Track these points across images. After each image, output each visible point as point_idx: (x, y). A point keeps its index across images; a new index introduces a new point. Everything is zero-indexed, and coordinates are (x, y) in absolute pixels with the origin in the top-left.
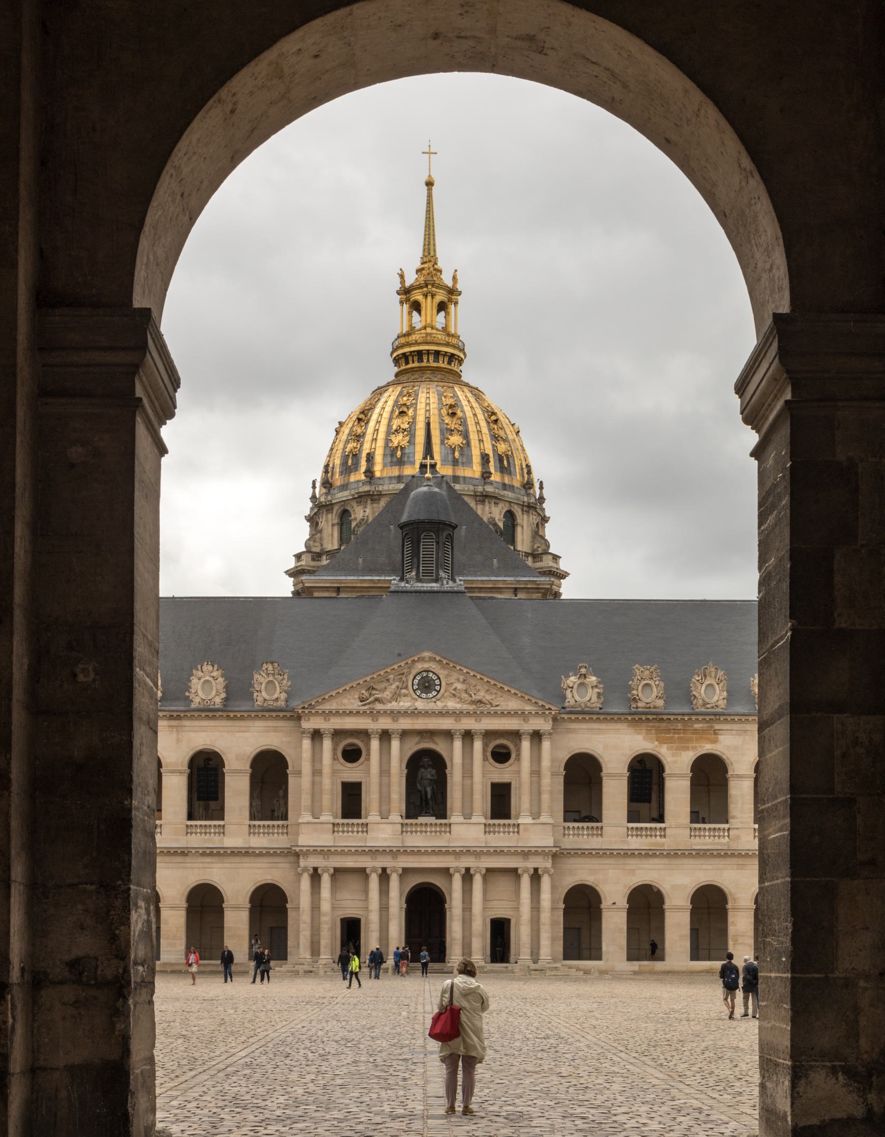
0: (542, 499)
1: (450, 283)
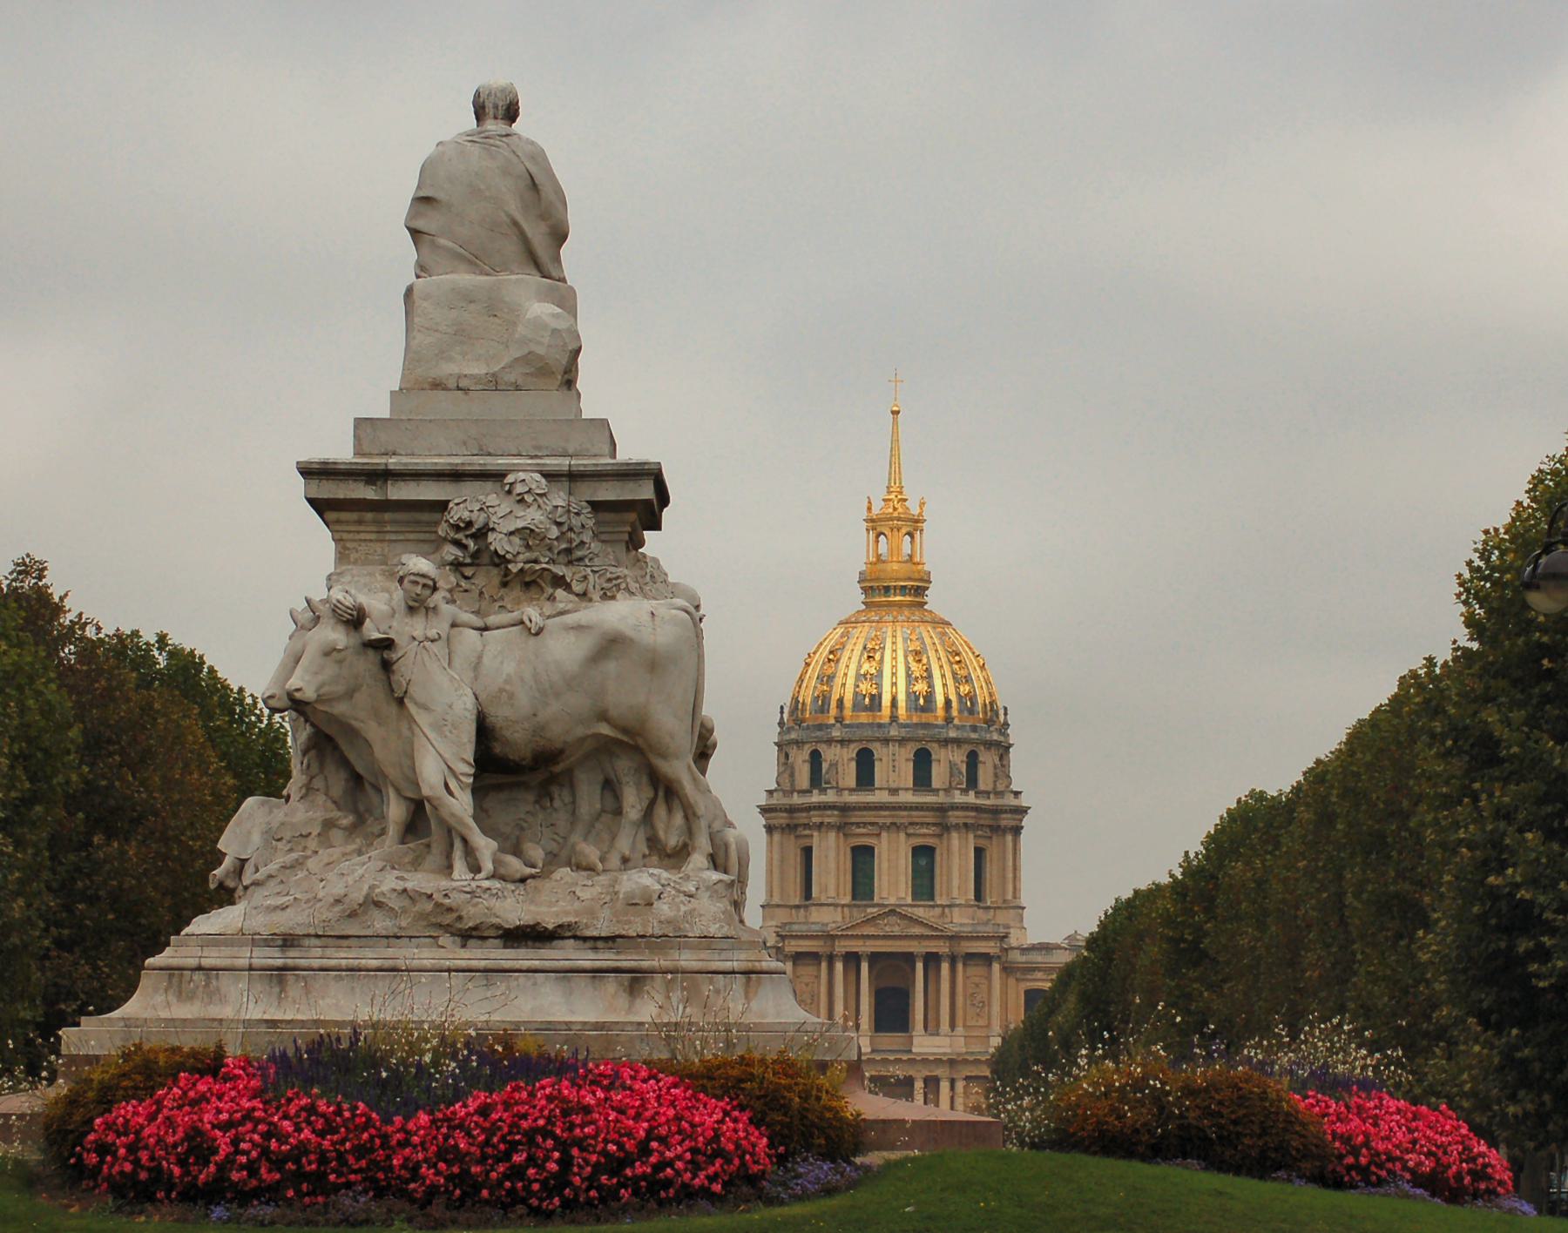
0: (1006, 725)
1: (915, 511)
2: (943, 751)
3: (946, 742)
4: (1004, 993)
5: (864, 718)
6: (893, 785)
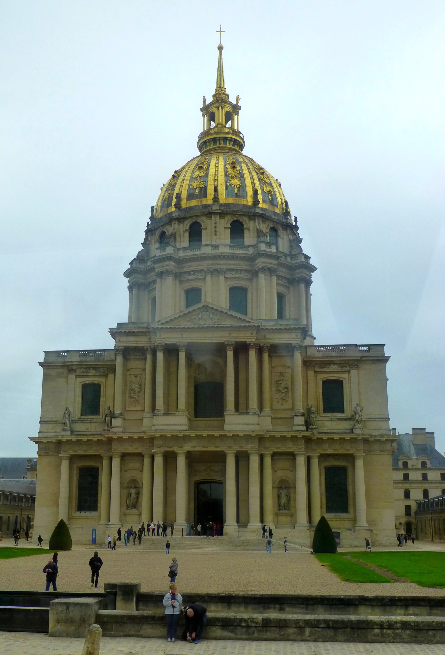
0: (296, 228)
1: (235, 103)
2: (252, 223)
4: (306, 382)
6: (214, 242)
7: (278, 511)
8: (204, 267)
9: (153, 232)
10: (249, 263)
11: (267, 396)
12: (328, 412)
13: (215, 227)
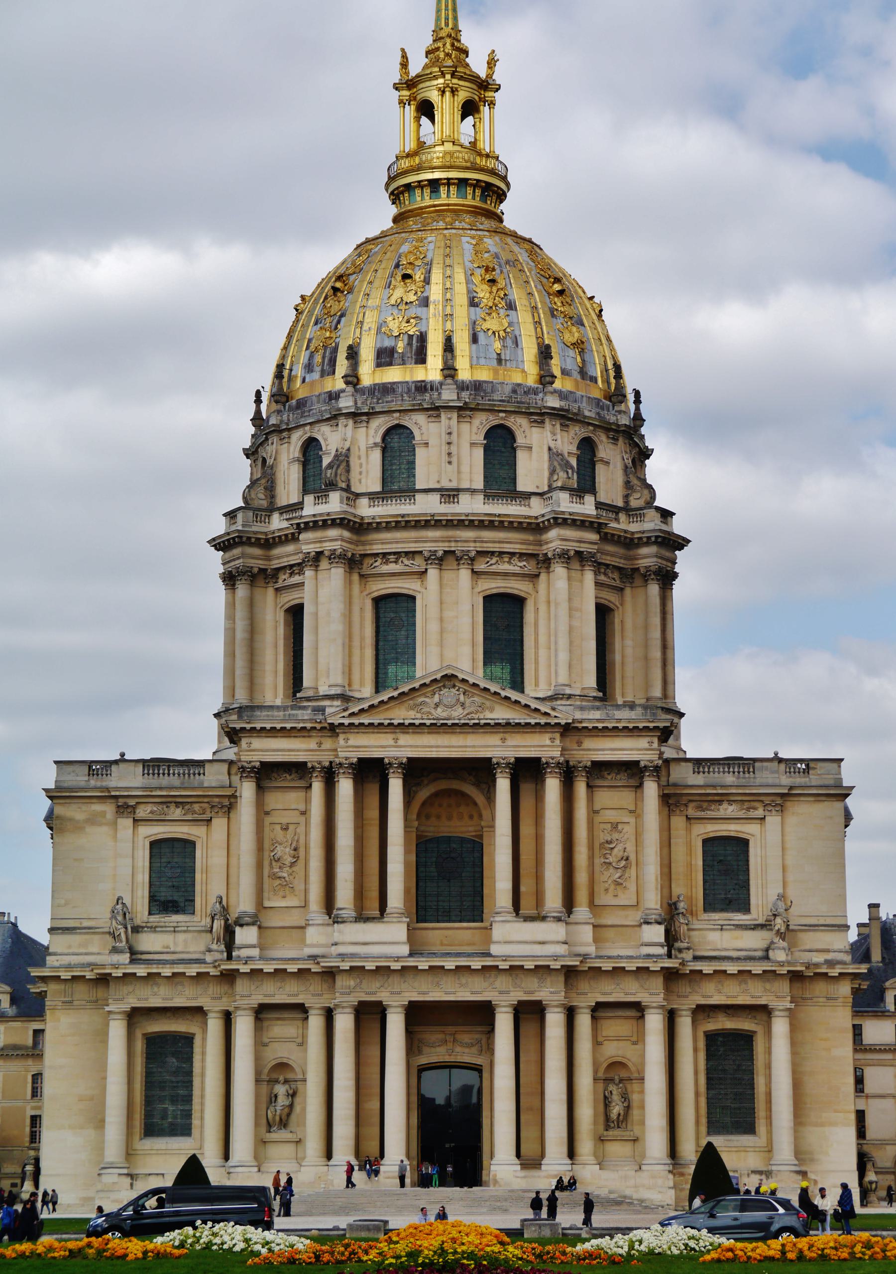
0: (639, 419)
1: (482, 73)
3: (539, 416)
4: (666, 843)
5: (393, 375)
6: (446, 484)
7: (605, 1133)
8: (421, 545)
9: (285, 434)
10: (531, 538)
11: (581, 878)
12: (714, 910)
13: (449, 443)
